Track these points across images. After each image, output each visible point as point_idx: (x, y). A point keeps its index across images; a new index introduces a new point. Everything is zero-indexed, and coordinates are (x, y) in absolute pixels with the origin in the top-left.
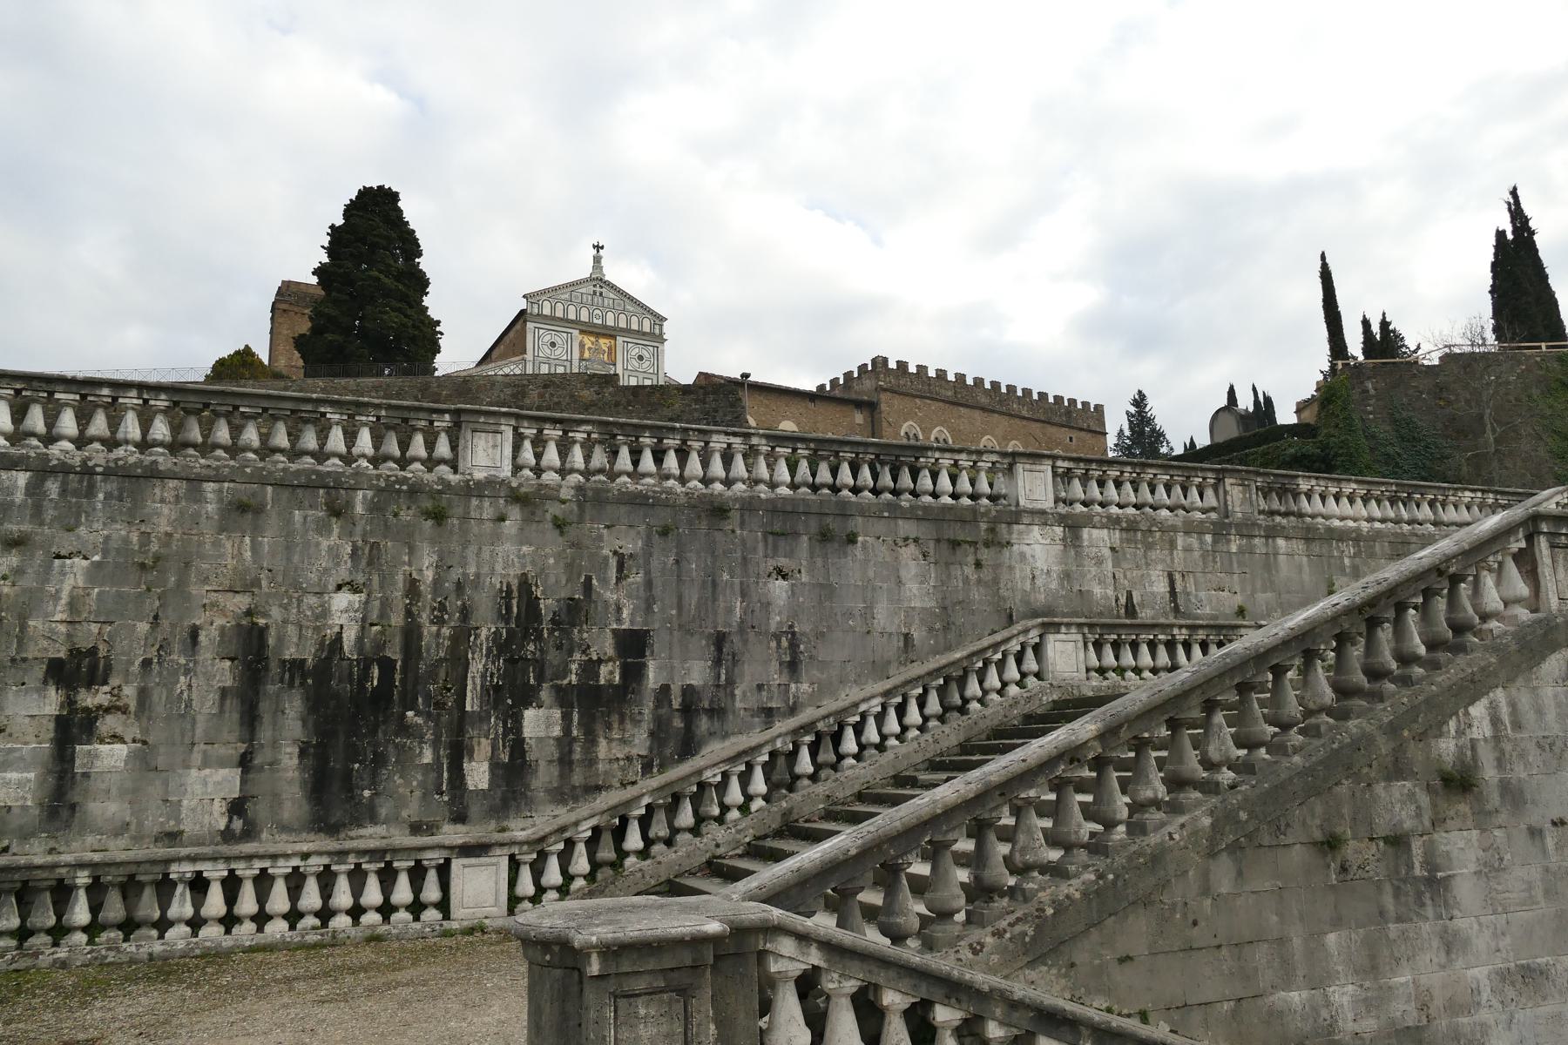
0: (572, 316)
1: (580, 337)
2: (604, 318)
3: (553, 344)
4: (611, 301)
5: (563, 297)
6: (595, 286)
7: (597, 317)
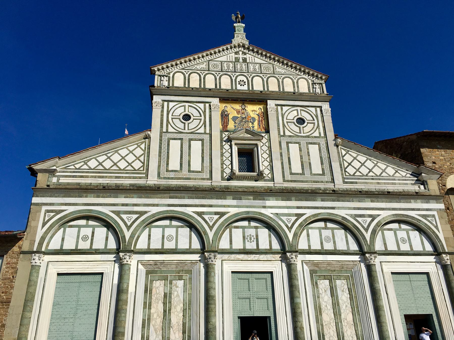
0: (210, 84)
1: (222, 106)
2: (250, 83)
3: (187, 117)
4: (257, 67)
5: (198, 67)
7: (242, 83)
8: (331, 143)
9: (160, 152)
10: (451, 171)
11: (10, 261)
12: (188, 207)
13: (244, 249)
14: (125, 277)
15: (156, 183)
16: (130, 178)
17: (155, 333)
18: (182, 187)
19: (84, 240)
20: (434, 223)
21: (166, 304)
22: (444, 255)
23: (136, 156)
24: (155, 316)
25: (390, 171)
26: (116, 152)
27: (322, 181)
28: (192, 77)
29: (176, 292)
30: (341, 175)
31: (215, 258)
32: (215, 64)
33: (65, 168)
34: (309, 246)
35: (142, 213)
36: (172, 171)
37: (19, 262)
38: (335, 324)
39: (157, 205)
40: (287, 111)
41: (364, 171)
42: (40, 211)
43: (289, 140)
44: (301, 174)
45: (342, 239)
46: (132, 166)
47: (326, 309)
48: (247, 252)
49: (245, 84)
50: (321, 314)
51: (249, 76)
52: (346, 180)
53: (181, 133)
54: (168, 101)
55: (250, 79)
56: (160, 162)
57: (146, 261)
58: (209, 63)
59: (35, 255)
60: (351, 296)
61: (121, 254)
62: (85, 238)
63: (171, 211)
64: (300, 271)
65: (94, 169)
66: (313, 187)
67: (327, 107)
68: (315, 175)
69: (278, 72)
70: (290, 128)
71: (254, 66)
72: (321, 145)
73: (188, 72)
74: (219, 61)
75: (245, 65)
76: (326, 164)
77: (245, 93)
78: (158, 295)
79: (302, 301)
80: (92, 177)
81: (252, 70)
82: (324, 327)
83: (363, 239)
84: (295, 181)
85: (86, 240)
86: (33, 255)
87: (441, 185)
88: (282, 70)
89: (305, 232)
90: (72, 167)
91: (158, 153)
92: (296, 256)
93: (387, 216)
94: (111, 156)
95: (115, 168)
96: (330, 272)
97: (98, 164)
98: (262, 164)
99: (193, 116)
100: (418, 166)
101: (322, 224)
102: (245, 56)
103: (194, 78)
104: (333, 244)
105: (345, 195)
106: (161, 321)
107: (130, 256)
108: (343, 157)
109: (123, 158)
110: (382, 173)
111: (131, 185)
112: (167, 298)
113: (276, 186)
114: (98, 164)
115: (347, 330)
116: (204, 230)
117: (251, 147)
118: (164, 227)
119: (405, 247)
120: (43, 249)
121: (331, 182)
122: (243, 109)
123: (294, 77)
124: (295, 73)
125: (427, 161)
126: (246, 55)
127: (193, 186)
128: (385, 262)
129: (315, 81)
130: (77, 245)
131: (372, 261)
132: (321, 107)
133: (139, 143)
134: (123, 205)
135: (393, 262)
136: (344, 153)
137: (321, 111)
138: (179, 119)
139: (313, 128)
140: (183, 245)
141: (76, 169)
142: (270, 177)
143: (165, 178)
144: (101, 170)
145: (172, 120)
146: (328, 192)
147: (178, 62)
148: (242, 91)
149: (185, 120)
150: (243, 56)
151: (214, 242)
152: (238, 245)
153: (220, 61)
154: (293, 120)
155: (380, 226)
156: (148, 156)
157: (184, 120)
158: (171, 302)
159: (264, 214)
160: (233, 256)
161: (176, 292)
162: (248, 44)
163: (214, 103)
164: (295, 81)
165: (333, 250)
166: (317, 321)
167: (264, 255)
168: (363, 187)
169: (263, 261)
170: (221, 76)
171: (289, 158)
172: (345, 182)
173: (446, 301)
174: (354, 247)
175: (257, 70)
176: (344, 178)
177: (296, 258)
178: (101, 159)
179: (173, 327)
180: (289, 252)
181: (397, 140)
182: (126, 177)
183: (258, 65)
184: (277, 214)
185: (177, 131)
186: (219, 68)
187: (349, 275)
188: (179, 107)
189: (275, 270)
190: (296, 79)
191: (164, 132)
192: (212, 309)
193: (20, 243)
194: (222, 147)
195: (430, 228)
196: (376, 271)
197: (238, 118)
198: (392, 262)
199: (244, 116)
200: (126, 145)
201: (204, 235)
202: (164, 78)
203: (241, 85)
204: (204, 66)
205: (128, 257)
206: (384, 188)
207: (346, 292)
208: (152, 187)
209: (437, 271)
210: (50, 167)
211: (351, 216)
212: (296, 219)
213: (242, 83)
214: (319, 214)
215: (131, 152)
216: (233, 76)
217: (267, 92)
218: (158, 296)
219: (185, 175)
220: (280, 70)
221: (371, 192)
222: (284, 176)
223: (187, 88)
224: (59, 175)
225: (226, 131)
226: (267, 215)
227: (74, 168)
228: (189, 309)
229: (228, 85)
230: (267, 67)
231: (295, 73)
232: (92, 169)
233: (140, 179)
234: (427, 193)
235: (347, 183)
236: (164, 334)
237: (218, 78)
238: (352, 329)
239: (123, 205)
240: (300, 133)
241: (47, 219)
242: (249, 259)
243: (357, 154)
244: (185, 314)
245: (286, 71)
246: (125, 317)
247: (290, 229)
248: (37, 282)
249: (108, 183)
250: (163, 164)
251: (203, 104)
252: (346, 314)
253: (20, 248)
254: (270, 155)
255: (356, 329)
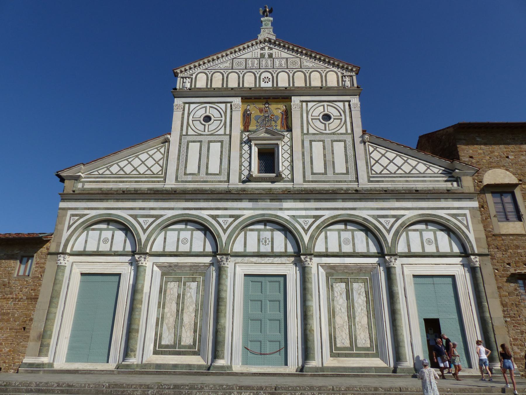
0: (233, 83)
2: (275, 79)
3: (207, 119)
4: (283, 62)
5: (222, 66)
6: (262, 49)
8: (358, 140)
9: (179, 156)
10: (490, 166)
11: (39, 261)
12: (203, 210)
13: (258, 252)
14: (140, 278)
15: (174, 186)
16: (148, 182)
17: (168, 331)
18: (199, 190)
19: (104, 242)
20: (465, 222)
21: (179, 304)
22: (472, 257)
23: (155, 161)
24: (168, 315)
25: (421, 167)
26: (137, 156)
27: (345, 181)
28: (215, 77)
29: (189, 294)
30: (366, 173)
31: (227, 261)
32: (239, 62)
33: (90, 174)
34: (327, 249)
35: (157, 217)
36: (190, 174)
37: (48, 263)
38: (348, 327)
39: (173, 209)
40: (312, 107)
41: (392, 168)
42: (66, 215)
43: (313, 138)
44: (322, 174)
45: (362, 241)
46: (151, 171)
47: (340, 311)
48: (261, 255)
49: (270, 81)
50: (334, 317)
51: (275, 72)
52: (371, 179)
53: (201, 135)
54: (189, 103)
55: (275, 75)
56: (178, 165)
57: (161, 263)
58: (233, 61)
59: (60, 256)
60: (368, 299)
61: (137, 257)
62: (106, 241)
63: (186, 214)
64: (314, 274)
65: (116, 174)
66: (335, 187)
67: (356, 100)
68: (338, 174)
69: (306, 66)
70: (315, 126)
71: (280, 61)
72: (347, 142)
73: (211, 72)
74: (243, 58)
75: (270, 61)
76: (351, 162)
77: (268, 90)
78: (172, 296)
79: (313, 304)
80: (114, 182)
81: (277, 65)
82: (337, 330)
83: (384, 241)
84: (316, 182)
85: (106, 242)
86: (59, 255)
87: (476, 182)
88: (310, 64)
89: (323, 235)
90: (96, 173)
91: (176, 157)
92: (311, 259)
93: (412, 216)
94: (132, 161)
95: (135, 172)
96: (348, 276)
97: (120, 169)
98: (282, 165)
99: (214, 117)
100: (452, 161)
101: (342, 227)
102: (271, 52)
103: (216, 77)
104: (352, 246)
105: (368, 195)
106: (174, 320)
107: (145, 258)
108: (370, 154)
109: (143, 162)
110: (412, 170)
111: (149, 189)
112: (180, 299)
113: (295, 188)
114: (120, 169)
115: (360, 333)
116: (217, 234)
117: (272, 147)
118: (179, 230)
119: (430, 249)
120: (68, 250)
121: (355, 182)
122: (267, 108)
123: (322, 70)
124: (324, 66)
125: (463, 156)
126: (272, 50)
127: (209, 189)
128: (407, 264)
129: (345, 73)
130: (98, 248)
131: (392, 264)
132: (349, 101)
133: (158, 147)
134: (140, 209)
135: (416, 264)
136: (371, 149)
137: (349, 105)
138: (200, 121)
139: (340, 124)
140: (198, 247)
141: (100, 174)
142: (290, 178)
143: (182, 182)
144: (122, 175)
145: (192, 122)
146: (350, 192)
147: (201, 63)
148: (265, 89)
149: (206, 121)
150: (269, 52)
151: (227, 245)
152: (252, 248)
153: (245, 58)
154: (319, 116)
155: (404, 227)
156: (167, 160)
157: (204, 122)
158: (184, 303)
159: (280, 216)
160: (247, 258)
161: (189, 294)
162: (275, 39)
163: (236, 103)
164: (324, 75)
165: (351, 253)
166: (330, 324)
167: (279, 258)
168: (390, 186)
169: (277, 264)
170: (245, 74)
171: (311, 158)
172: (370, 181)
173: (471, 306)
174: (373, 249)
175: (283, 65)
176: (369, 177)
177: (311, 261)
178: (122, 164)
179: (185, 326)
180: (303, 255)
181: (437, 133)
182: (145, 182)
183: (284, 60)
184: (294, 216)
185: (197, 134)
186: (243, 65)
187: (368, 278)
188: (200, 109)
189: (289, 273)
190: (325, 72)
191: (184, 135)
192: (221, 311)
193: (48, 244)
194: (241, 148)
195: (460, 228)
196: (395, 274)
197: (260, 117)
198: (414, 264)
199: (267, 115)
200: (147, 149)
201: (218, 238)
202: (186, 80)
203: (265, 82)
204: (228, 65)
205: (143, 259)
206: (412, 186)
207: (362, 295)
208: (169, 191)
209: (464, 274)
210: (76, 173)
211: (373, 217)
212: (313, 221)
213: (267, 80)
214: (339, 215)
215: (151, 156)
216: (258, 73)
217: (292, 88)
218: (172, 297)
219: (202, 178)
220: (308, 64)
221: (397, 191)
222: (304, 177)
223: (209, 88)
224: (84, 181)
225: (248, 131)
226: (283, 218)
227: (98, 174)
228: (201, 309)
229: (252, 83)
230: (294, 61)
231: (324, 66)
232: (114, 175)
233: (158, 183)
234: (460, 190)
235: (372, 182)
236: (177, 332)
237: (241, 76)
238: (366, 333)
239: (140, 209)
240: (325, 130)
241: (71, 222)
242: (263, 262)
243: (385, 150)
244: (197, 315)
245: (314, 65)
246: (140, 315)
247: (306, 231)
248: (63, 281)
249: (127, 188)
250: (181, 167)
251: (224, 105)
252: (360, 317)
253: (48, 249)
254: (292, 155)
255: (371, 332)
